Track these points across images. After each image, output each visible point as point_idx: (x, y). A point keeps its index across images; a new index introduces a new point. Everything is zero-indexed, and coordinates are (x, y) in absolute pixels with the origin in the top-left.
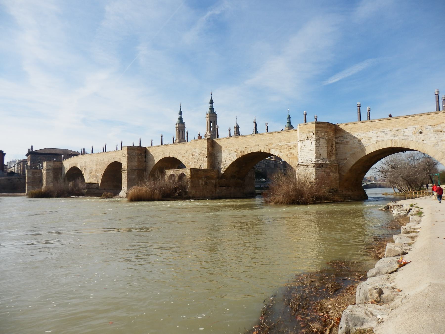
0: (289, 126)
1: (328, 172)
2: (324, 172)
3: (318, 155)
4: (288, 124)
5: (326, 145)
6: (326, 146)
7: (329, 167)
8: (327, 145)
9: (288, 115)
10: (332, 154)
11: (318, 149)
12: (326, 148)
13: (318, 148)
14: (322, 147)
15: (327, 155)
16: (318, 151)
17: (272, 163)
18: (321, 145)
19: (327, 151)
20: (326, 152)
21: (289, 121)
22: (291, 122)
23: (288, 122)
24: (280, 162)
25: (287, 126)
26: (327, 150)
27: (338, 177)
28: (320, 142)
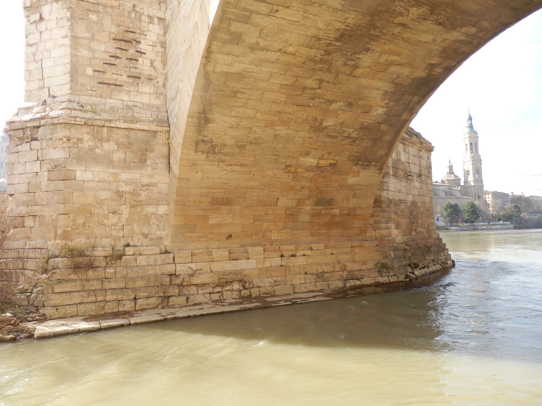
0: (470, 132)
1: (56, 166)
2: (39, 162)
3: (35, 85)
4: (468, 129)
5: (66, 31)
6: (66, 36)
7: (61, 133)
8: (72, 28)
9: (468, 115)
10: (124, 78)
11: (34, 55)
12: (67, 41)
13: (32, 49)
14: (49, 45)
15: (67, 78)
16: (33, 66)
17: (442, 189)
18: (45, 36)
19: (67, 60)
20: (65, 64)
21: (470, 124)
22: (473, 125)
23: (468, 125)
24: (455, 188)
25: (467, 132)
26: (68, 51)
27: (163, 187)
28: (41, 18)
